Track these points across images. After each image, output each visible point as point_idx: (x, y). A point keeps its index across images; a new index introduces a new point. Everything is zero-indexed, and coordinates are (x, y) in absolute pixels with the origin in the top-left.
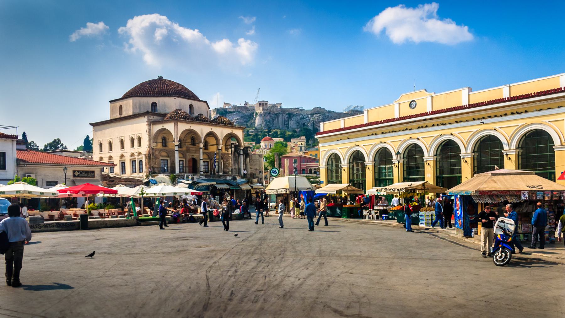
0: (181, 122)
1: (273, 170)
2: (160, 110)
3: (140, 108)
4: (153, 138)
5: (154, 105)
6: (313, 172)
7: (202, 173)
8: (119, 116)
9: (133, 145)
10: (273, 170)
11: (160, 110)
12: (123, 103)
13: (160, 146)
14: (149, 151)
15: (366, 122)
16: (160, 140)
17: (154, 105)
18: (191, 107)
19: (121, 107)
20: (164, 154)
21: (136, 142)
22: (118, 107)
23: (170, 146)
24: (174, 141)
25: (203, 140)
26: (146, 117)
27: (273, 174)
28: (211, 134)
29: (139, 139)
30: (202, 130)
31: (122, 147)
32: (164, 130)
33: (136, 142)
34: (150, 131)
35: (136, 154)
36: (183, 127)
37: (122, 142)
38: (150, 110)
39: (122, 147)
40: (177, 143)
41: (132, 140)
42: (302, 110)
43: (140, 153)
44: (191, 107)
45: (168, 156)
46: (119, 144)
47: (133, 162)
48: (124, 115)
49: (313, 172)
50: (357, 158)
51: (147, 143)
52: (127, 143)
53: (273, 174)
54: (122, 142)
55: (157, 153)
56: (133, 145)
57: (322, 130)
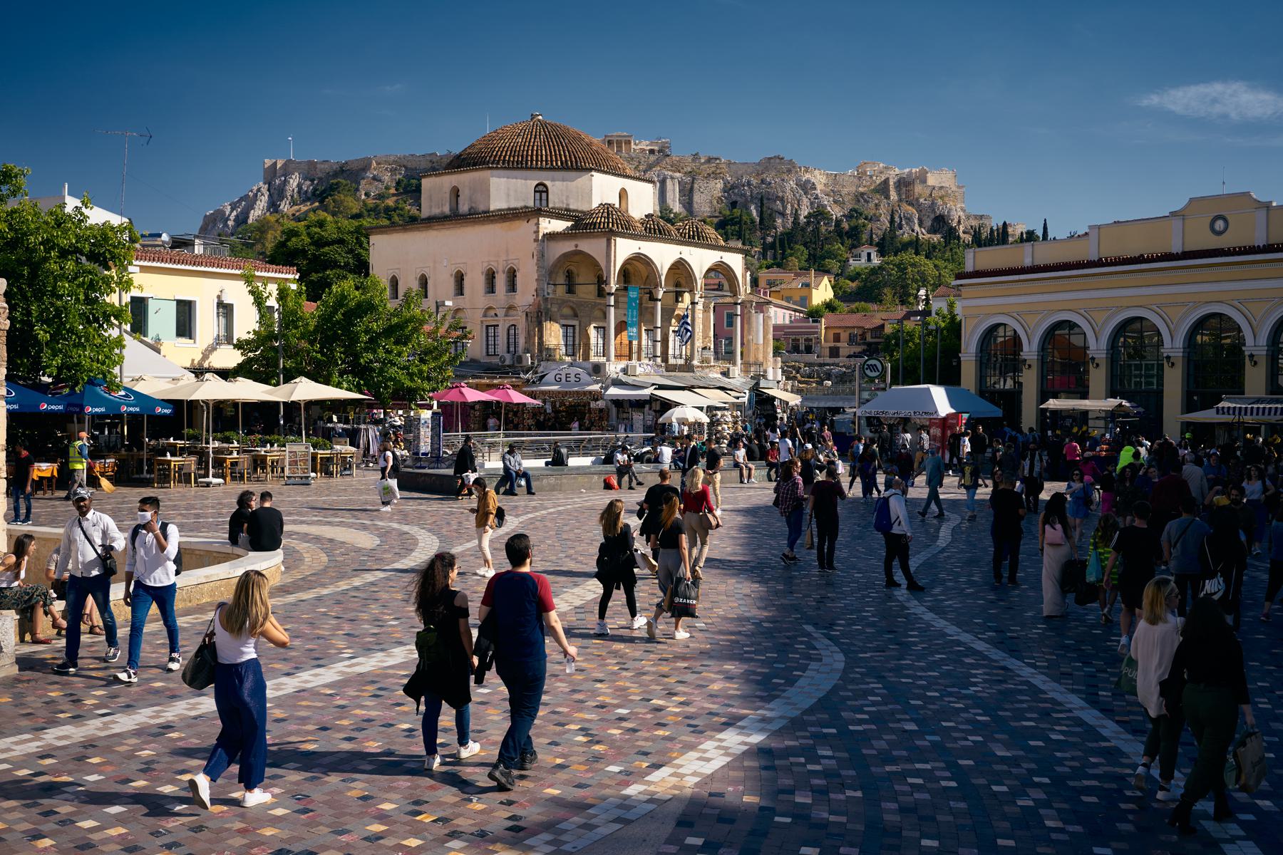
0: (623, 236)
1: (870, 362)
2: (555, 201)
3: (508, 195)
4: (549, 273)
5: (541, 190)
6: (802, 347)
7: (659, 360)
8: (447, 210)
9: (491, 288)
10: (870, 362)
11: (555, 201)
12: (463, 179)
13: (561, 290)
14: (539, 305)
15: (1094, 257)
16: (561, 279)
17: (541, 190)
18: (623, 194)
19: (456, 193)
20: (566, 311)
21: (501, 282)
22: (448, 191)
23: (586, 292)
24: (607, 282)
25: (663, 278)
26: (533, 221)
27: (868, 372)
28: (680, 269)
29: (512, 275)
30: (663, 255)
31: (460, 290)
32: (578, 253)
33: (501, 282)
34: (542, 255)
35: (501, 313)
36: (624, 249)
37: (460, 279)
38: (531, 204)
39: (460, 290)
40: (613, 286)
41: (491, 277)
42: (729, 164)
43: (511, 308)
44: (623, 194)
45: (576, 316)
46: (451, 285)
47: (490, 329)
48: (464, 208)
49: (802, 347)
50: (1060, 338)
51: (534, 285)
52: (476, 282)
53: (868, 372)
54: (460, 279)
55: (555, 309)
56: (491, 288)
57: (969, 267)
